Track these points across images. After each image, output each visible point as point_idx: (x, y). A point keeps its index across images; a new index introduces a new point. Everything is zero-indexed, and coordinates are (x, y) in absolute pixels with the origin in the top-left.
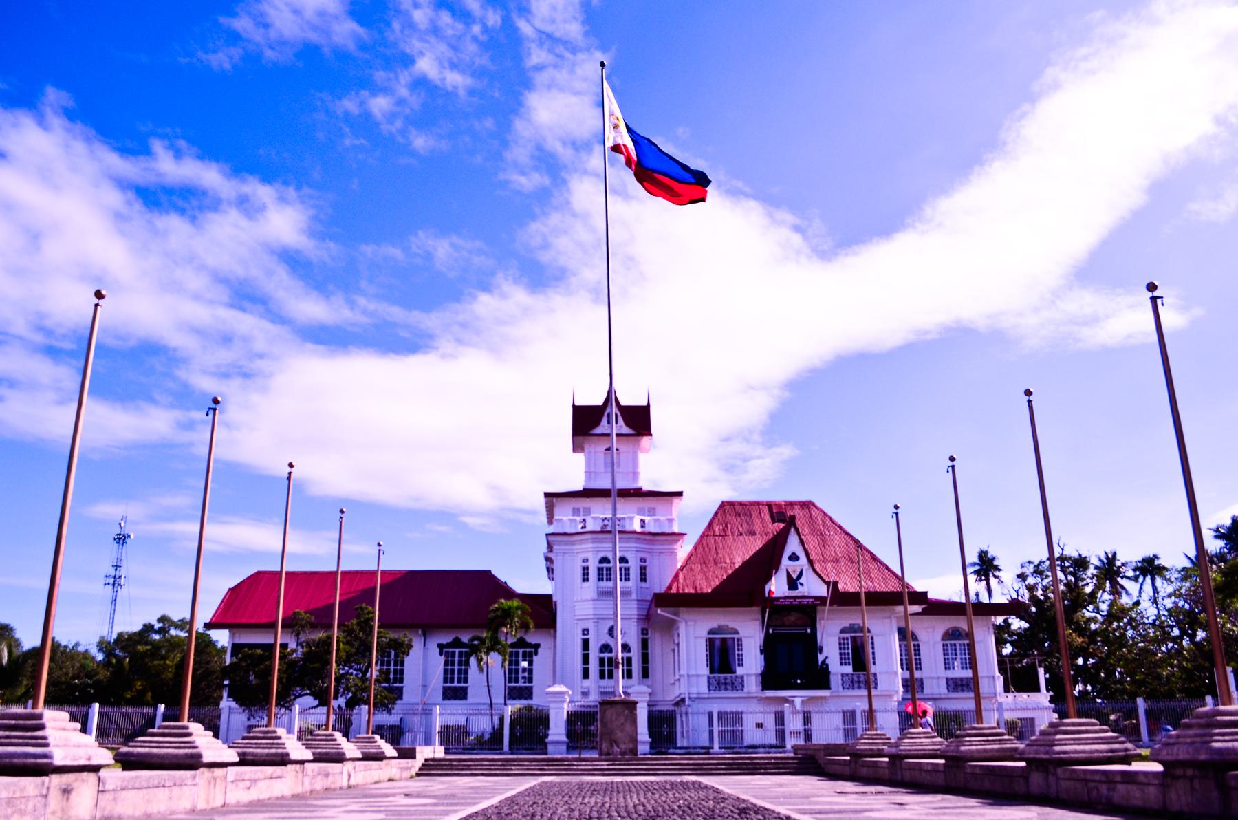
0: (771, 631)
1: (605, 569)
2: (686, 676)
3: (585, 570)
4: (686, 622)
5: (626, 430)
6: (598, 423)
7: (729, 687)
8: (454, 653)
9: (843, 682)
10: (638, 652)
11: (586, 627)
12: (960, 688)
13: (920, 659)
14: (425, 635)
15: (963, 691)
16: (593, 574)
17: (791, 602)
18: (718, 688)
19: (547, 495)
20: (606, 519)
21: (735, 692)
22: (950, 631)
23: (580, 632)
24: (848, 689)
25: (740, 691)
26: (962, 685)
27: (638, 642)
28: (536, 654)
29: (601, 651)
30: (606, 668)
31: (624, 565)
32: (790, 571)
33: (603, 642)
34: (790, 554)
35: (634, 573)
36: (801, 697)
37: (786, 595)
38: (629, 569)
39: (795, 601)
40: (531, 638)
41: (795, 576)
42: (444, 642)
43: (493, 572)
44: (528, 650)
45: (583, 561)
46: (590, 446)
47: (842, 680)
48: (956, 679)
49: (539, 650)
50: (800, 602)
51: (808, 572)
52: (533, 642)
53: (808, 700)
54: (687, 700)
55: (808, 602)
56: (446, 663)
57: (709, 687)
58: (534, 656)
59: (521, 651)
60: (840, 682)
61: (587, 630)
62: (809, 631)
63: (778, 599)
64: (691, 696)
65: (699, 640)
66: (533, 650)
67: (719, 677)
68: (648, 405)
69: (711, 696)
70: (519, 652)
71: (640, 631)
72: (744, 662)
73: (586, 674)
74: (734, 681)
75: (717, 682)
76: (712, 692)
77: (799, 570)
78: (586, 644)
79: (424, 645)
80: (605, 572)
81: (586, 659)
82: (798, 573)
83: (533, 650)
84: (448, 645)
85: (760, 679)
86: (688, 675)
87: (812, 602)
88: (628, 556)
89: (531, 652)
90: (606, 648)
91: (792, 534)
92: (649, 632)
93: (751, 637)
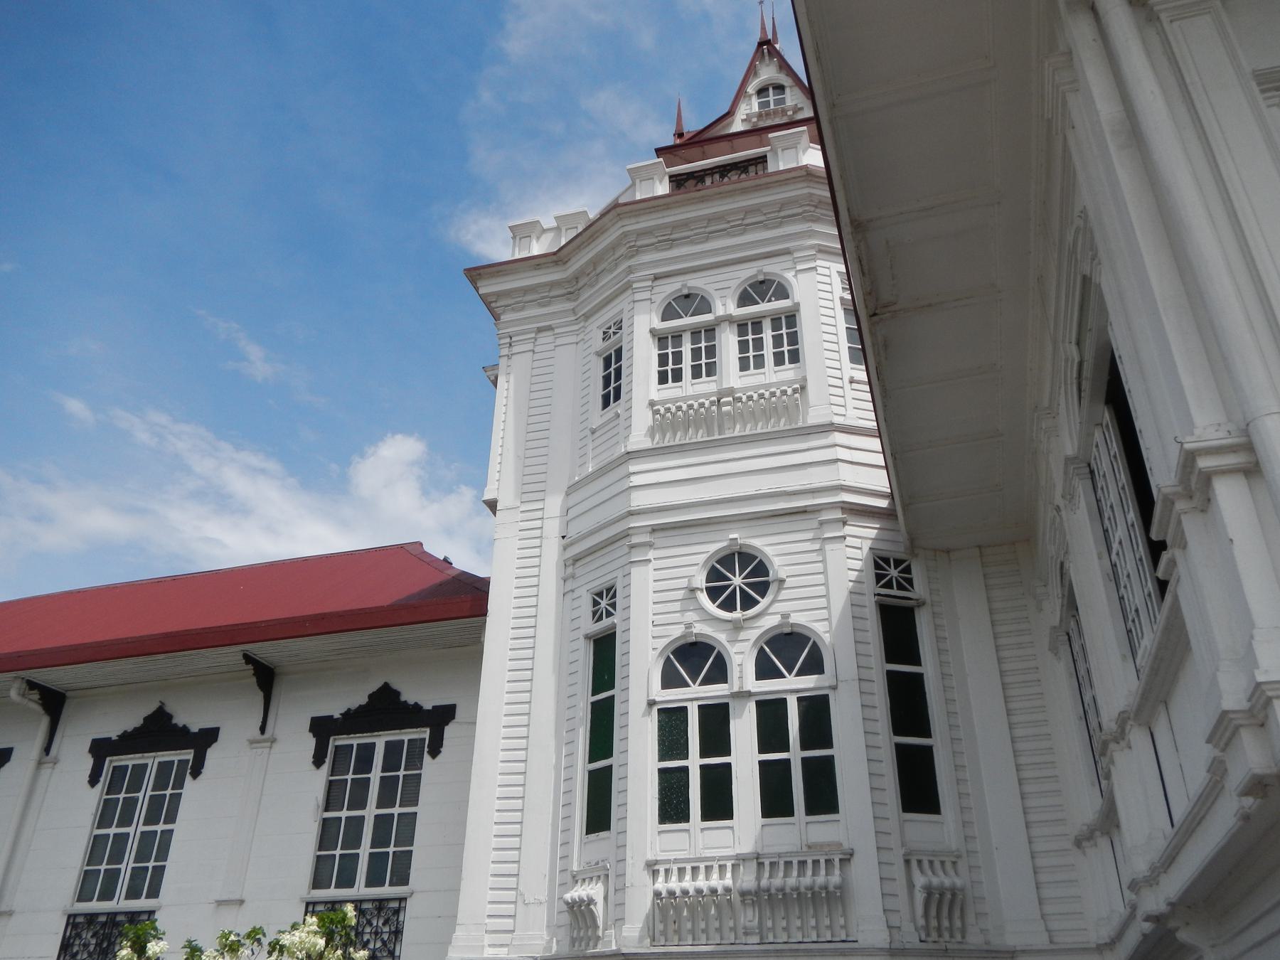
1: (687, 338)
11: (600, 583)
23: (587, 608)
28: (435, 751)
29: (671, 679)
30: (694, 762)
33: (677, 631)
44: (406, 735)
45: (606, 336)
49: (450, 731)
52: (428, 706)
58: (427, 757)
59: (380, 741)
79: (47, 750)
80: (687, 349)
83: (425, 734)
89: (415, 745)
92: (917, 574)
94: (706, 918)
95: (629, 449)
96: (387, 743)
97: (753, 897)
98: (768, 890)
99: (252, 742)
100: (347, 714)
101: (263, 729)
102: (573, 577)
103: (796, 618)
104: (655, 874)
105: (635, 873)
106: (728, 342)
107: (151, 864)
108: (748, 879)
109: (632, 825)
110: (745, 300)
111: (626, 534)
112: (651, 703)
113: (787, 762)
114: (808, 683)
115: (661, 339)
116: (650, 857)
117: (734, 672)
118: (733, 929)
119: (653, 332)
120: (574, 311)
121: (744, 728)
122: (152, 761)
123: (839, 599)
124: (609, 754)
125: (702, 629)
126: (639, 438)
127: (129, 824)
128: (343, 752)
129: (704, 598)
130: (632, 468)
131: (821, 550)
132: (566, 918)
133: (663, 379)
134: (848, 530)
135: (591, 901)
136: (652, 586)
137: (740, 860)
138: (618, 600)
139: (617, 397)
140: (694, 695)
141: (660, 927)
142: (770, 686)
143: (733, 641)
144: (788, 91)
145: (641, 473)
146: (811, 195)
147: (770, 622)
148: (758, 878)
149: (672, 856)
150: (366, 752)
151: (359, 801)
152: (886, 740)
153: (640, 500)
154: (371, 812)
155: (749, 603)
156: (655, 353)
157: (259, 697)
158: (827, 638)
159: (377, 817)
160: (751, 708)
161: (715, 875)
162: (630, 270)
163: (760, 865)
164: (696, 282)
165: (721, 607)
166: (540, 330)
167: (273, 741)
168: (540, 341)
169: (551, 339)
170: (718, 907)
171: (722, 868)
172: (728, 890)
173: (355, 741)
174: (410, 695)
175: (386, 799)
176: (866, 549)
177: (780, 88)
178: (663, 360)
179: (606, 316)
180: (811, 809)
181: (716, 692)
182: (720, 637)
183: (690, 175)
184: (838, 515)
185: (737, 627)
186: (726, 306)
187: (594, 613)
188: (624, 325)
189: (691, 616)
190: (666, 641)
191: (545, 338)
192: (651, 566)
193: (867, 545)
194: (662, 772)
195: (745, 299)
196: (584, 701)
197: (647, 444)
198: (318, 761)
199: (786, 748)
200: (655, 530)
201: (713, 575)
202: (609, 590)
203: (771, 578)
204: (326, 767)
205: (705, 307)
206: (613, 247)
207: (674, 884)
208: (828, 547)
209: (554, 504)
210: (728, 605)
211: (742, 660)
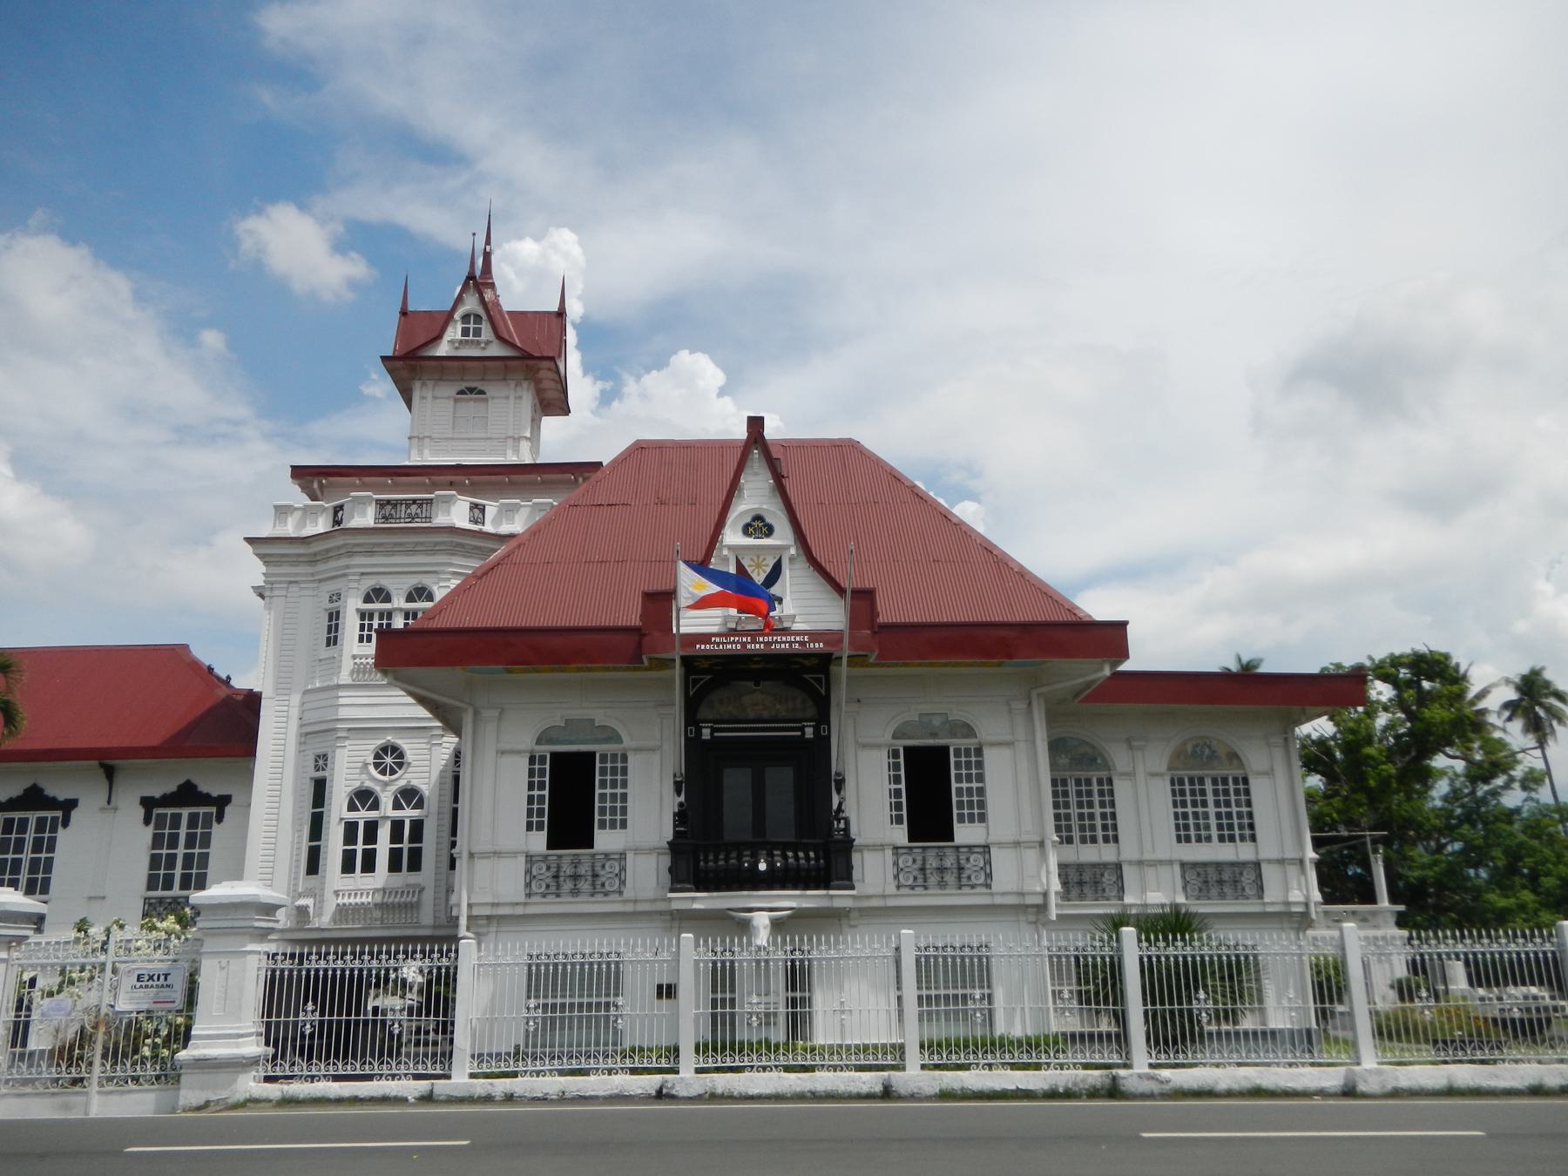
0: (706, 734)
1: (376, 616)
2: (465, 855)
3: (334, 617)
4: (476, 713)
6: (439, 337)
7: (585, 886)
8: (23, 824)
9: (900, 870)
11: (320, 751)
12: (1214, 891)
13: (1114, 815)
15: (1222, 896)
17: (744, 645)
18: (553, 889)
21: (599, 897)
22: (1189, 748)
23: (311, 763)
24: (912, 888)
25: (615, 897)
26: (1220, 882)
28: (220, 819)
29: (352, 807)
30: (360, 847)
32: (746, 563)
33: (357, 784)
34: (748, 520)
36: (771, 910)
37: (733, 626)
39: (754, 641)
41: (759, 577)
43: (192, 648)
44: (202, 810)
45: (331, 601)
46: (424, 384)
47: (896, 864)
48: (1205, 865)
49: (228, 809)
50: (770, 644)
51: (798, 566)
52: (215, 794)
53: (789, 917)
54: (463, 921)
55: (791, 643)
57: (528, 885)
58: (215, 824)
59: (185, 813)
60: (891, 871)
62: (809, 733)
63: (705, 638)
64: (475, 912)
65: (507, 760)
66: (214, 810)
67: (560, 857)
69: (531, 910)
70: (180, 815)
72: (629, 817)
73: (314, 864)
74: (598, 868)
75: (553, 870)
76: (534, 899)
77: (771, 562)
81: (317, 827)
82: (768, 570)
83: (214, 810)
85: (666, 861)
86: (471, 855)
87: (802, 644)
88: (426, 581)
89: (208, 816)
90: (364, 797)
91: (756, 465)
93: (653, 750)
94: (359, 914)
95: (340, 683)
96: (190, 814)
97: (381, 906)
98: (386, 904)
99: (102, 809)
100: (164, 797)
101: (109, 802)
102: (305, 743)
103: (415, 783)
104: (338, 896)
105: (329, 894)
107: (40, 876)
108: (378, 898)
109: (328, 874)
111: (335, 730)
112: (342, 819)
113: (402, 848)
114: (416, 813)
115: (363, 615)
116: (336, 889)
117: (382, 806)
118: (371, 919)
119: (358, 610)
120: (313, 575)
121: (384, 833)
122: (32, 817)
123: (435, 774)
124: (319, 839)
125: (369, 784)
126: (344, 677)
127: (22, 852)
128: (162, 817)
129: (371, 768)
130: (340, 694)
131: (430, 749)
132: (294, 912)
133: (361, 639)
134: (445, 739)
135: (307, 907)
136: (346, 759)
137: (376, 891)
138: (329, 762)
139: (335, 644)
140: (363, 815)
141: (338, 917)
142: (398, 814)
143: (383, 791)
144: (484, 323)
145: (346, 698)
146: (452, 542)
147: (402, 783)
148: (384, 897)
149: (346, 888)
151: (173, 843)
153: (344, 713)
154: (181, 851)
155: (393, 772)
156: (358, 622)
157: (106, 784)
158: (426, 793)
159: (185, 854)
160: (388, 825)
161: (364, 897)
162: (348, 567)
163: (385, 893)
164: (385, 582)
165: (380, 772)
166: (291, 582)
167: (116, 809)
168: (291, 589)
169: (297, 589)
170: (365, 910)
171: (368, 894)
172: (369, 903)
173: (169, 811)
174: (204, 787)
175: (190, 843)
176: (452, 749)
177: (478, 318)
178: (362, 628)
179: (332, 586)
180: (410, 869)
181: (373, 814)
182: (377, 789)
183: (389, 502)
184: (441, 732)
185: (386, 784)
187: (316, 766)
188: (342, 597)
189: (364, 776)
190: (351, 789)
191: (294, 588)
192: (346, 750)
193: (452, 747)
194: (344, 851)
195: (410, 599)
196: (308, 812)
197: (349, 681)
198: (147, 821)
199: (402, 843)
200: (350, 729)
201: (377, 756)
202: (324, 756)
203: (405, 760)
204: (151, 827)
205: (388, 599)
206: (339, 548)
207: (346, 901)
208: (433, 748)
209: (296, 699)
210: (383, 772)
211: (386, 800)
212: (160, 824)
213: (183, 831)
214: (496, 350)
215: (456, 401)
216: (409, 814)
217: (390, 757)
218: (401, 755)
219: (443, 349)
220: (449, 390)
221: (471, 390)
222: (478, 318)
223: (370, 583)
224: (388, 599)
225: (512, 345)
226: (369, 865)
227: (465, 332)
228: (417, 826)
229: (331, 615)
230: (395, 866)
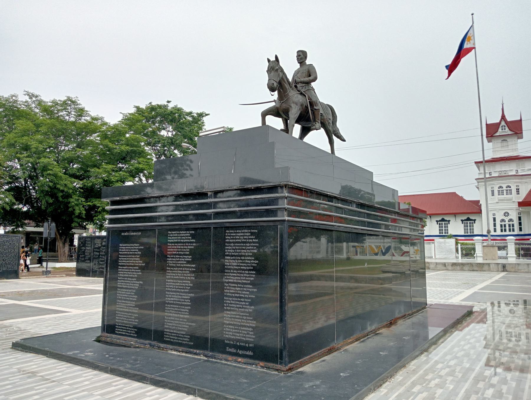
5: (510, 133)
6: (497, 131)
8: (442, 224)
10: (517, 222)
14: (430, 217)
16: (496, 193)
19: (476, 163)
20: (500, 171)
27: (517, 218)
28: (475, 223)
29: (501, 222)
31: (509, 189)
35: (514, 191)
38: (511, 190)
40: (472, 217)
42: (438, 220)
46: (494, 140)
49: (476, 221)
56: (440, 227)
59: (469, 222)
61: (495, 214)
66: (473, 221)
68: (521, 120)
71: (517, 214)
78: (494, 220)
84: (440, 221)
88: (510, 185)
90: (503, 220)
106: (505, 192)
110: (507, 188)
121: (507, 226)
125: (504, 218)
139: (494, 195)
140: (503, 223)
142: (509, 223)
147: (510, 218)
150: (467, 223)
151: (467, 226)
152: (518, 227)
155: (507, 216)
164: (501, 185)
181: (505, 223)
186: (505, 188)
198: (462, 223)
201: (504, 214)
210: (506, 216)
211: (507, 221)
212: (465, 223)
213: (469, 225)
214: (510, 132)
215: (501, 142)
216: (511, 223)
217: (506, 214)
218: (508, 214)
219: (497, 134)
220: (500, 141)
221: (504, 140)
222: (505, 126)
223: (499, 185)
224: (502, 188)
225: (514, 131)
226: (505, 231)
227: (502, 129)
228: (513, 225)
229: (492, 191)
230: (510, 230)
